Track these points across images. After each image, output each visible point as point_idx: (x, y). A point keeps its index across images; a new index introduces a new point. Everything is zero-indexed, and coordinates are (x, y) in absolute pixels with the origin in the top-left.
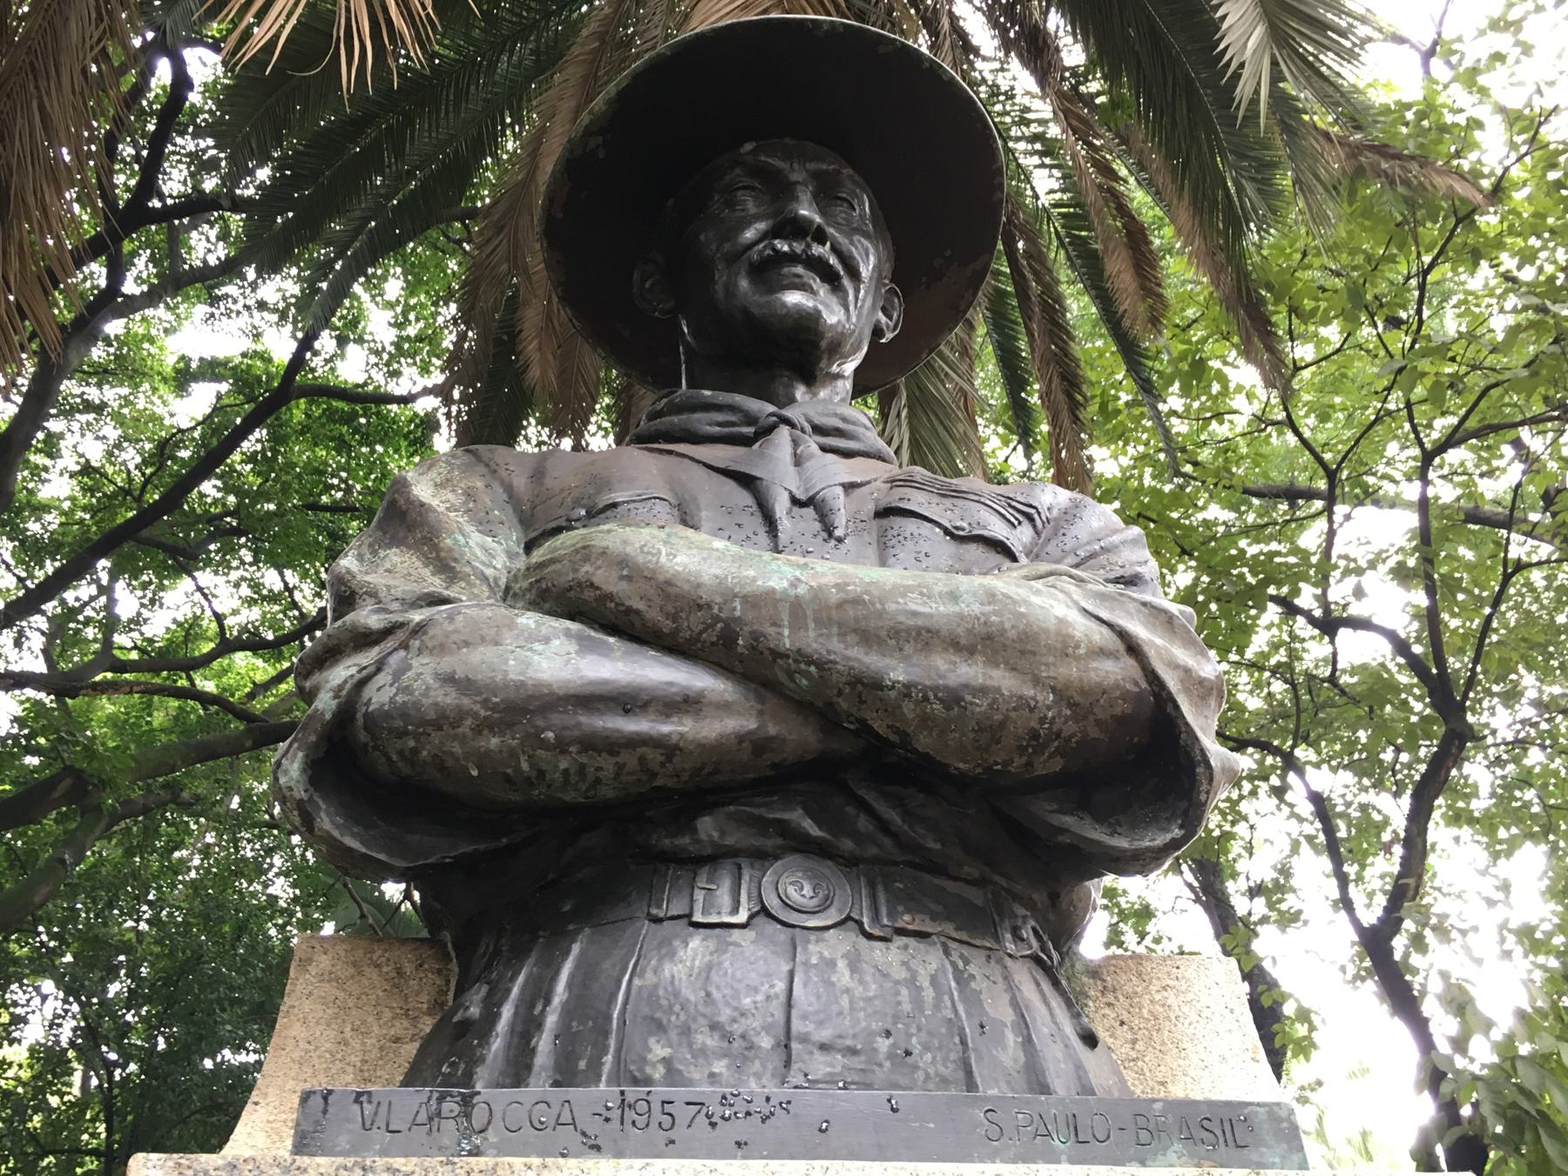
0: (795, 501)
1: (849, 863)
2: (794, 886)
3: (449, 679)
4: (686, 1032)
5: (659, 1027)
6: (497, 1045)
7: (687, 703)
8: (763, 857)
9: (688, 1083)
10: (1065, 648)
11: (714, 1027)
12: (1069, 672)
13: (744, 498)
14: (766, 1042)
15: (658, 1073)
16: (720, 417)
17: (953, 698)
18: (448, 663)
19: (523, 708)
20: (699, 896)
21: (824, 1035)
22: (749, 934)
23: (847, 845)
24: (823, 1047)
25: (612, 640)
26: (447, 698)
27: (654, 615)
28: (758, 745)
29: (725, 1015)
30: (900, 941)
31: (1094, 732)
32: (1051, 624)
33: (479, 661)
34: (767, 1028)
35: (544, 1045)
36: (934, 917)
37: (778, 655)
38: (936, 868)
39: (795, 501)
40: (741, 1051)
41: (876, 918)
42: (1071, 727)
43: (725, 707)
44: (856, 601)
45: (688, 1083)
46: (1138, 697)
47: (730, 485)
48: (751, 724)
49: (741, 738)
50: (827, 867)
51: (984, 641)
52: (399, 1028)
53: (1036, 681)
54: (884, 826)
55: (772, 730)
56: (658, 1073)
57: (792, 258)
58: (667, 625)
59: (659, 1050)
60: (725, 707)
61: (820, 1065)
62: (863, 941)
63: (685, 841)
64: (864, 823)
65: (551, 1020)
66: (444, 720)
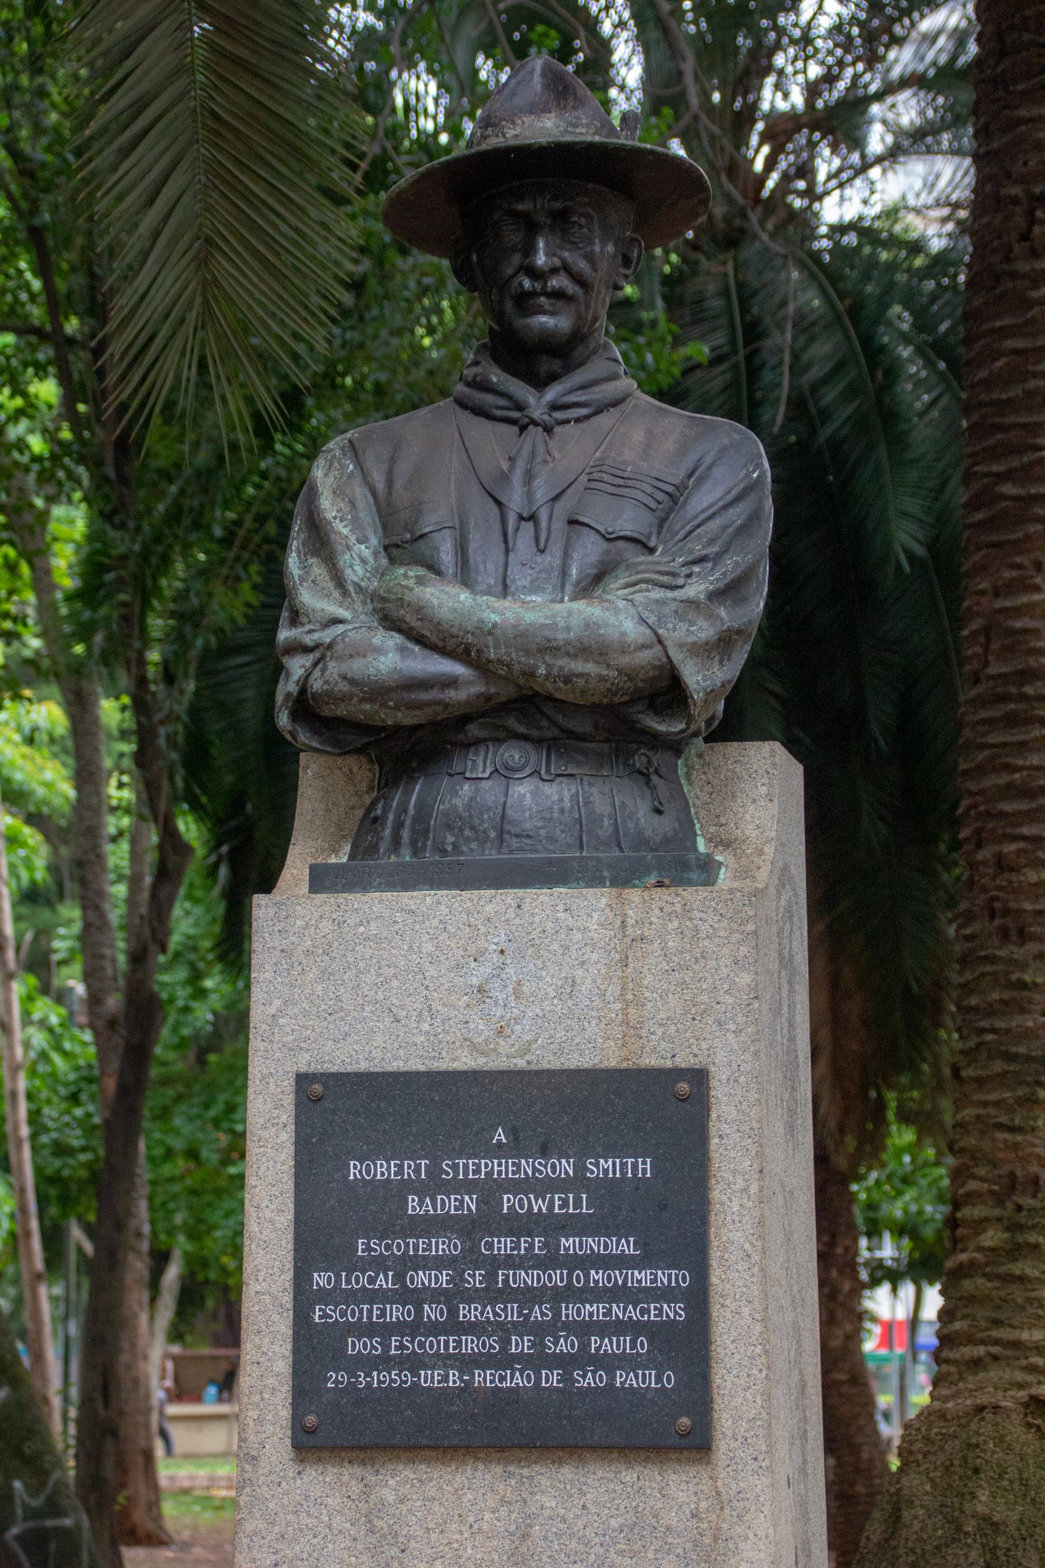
0: (521, 518)
1: (537, 742)
2: (512, 753)
3: (344, 678)
4: (461, 830)
5: (449, 827)
6: (387, 832)
7: (451, 682)
8: (498, 741)
9: (462, 853)
10: (624, 648)
11: (472, 828)
12: (624, 660)
13: (496, 511)
14: (493, 834)
15: (449, 848)
16: (501, 402)
17: (567, 680)
18: (344, 667)
19: (378, 691)
20: (469, 764)
21: (517, 830)
22: (490, 783)
23: (535, 733)
24: (517, 836)
25: (417, 648)
26: (344, 687)
27: (434, 639)
28: (488, 698)
29: (476, 821)
30: (559, 780)
31: (641, 684)
32: (615, 637)
33: (357, 667)
34: (494, 828)
35: (406, 834)
36: (578, 764)
37: (489, 661)
38: (582, 738)
39: (521, 518)
40: (483, 839)
41: (548, 771)
42: (629, 685)
43: (471, 683)
44: (523, 635)
45: (462, 853)
46: (660, 668)
47: (492, 504)
48: (482, 689)
49: (479, 696)
50: (528, 746)
51: (583, 650)
52: (354, 800)
53: (608, 666)
54: (554, 723)
55: (493, 690)
56: (449, 848)
57: (534, 294)
58: (440, 644)
59: (450, 839)
60: (471, 683)
61: (515, 843)
62: (541, 784)
63: (461, 737)
64: (545, 723)
65: (408, 823)
66: (345, 698)
